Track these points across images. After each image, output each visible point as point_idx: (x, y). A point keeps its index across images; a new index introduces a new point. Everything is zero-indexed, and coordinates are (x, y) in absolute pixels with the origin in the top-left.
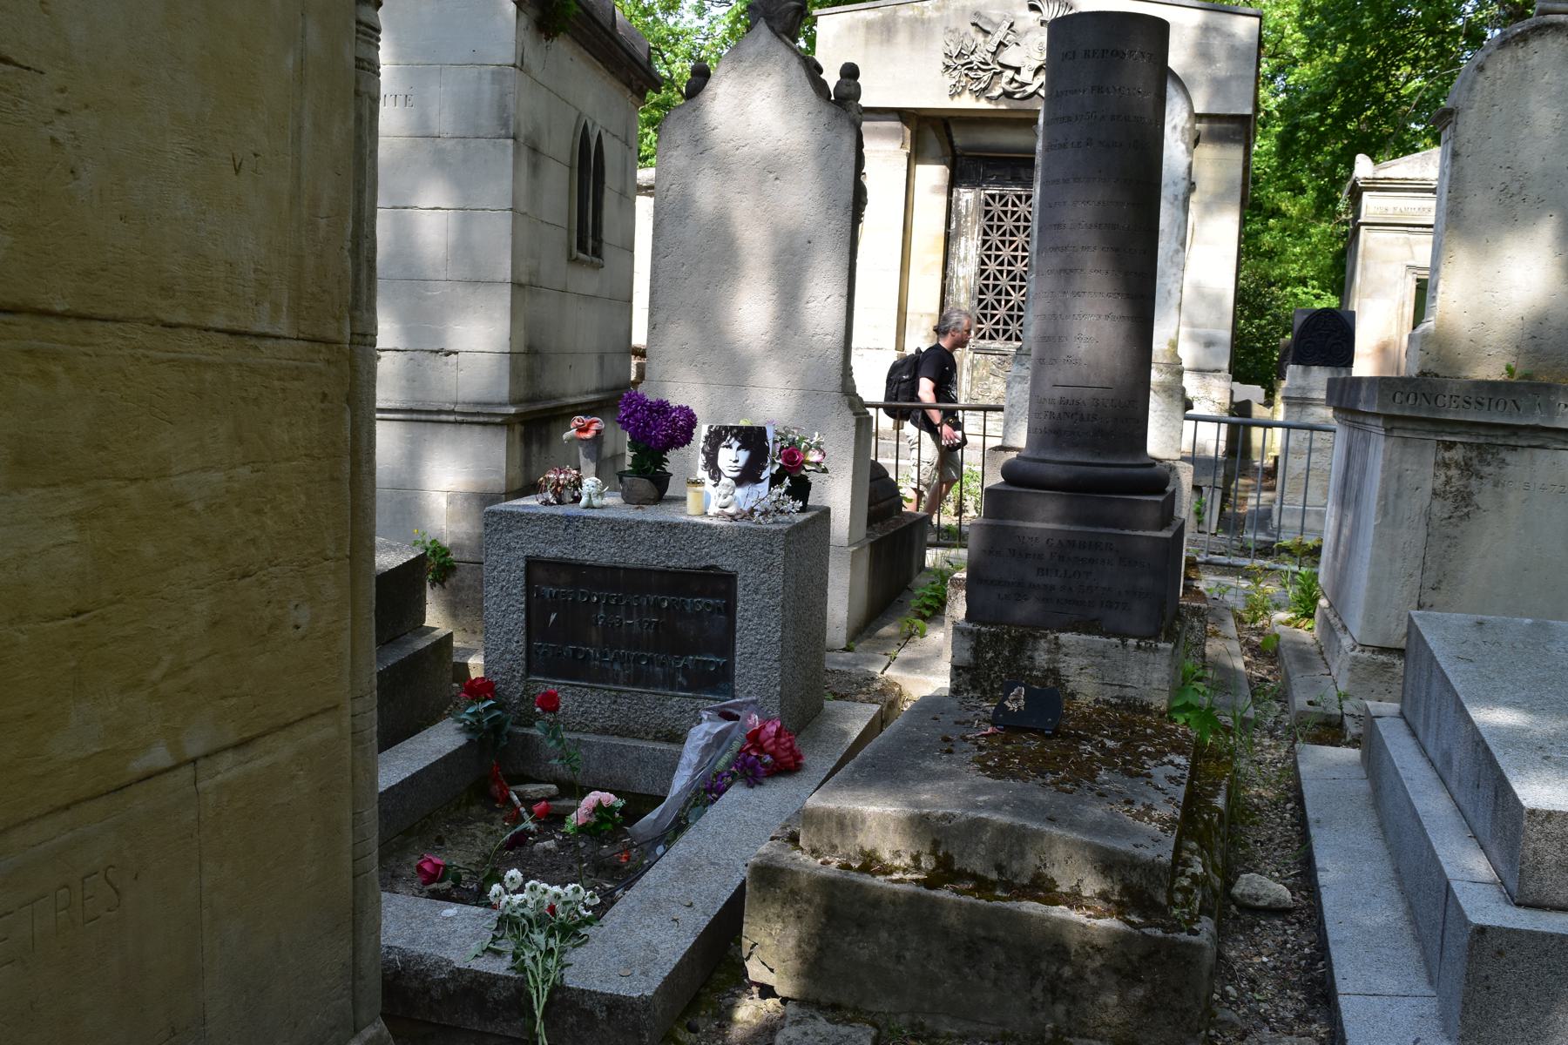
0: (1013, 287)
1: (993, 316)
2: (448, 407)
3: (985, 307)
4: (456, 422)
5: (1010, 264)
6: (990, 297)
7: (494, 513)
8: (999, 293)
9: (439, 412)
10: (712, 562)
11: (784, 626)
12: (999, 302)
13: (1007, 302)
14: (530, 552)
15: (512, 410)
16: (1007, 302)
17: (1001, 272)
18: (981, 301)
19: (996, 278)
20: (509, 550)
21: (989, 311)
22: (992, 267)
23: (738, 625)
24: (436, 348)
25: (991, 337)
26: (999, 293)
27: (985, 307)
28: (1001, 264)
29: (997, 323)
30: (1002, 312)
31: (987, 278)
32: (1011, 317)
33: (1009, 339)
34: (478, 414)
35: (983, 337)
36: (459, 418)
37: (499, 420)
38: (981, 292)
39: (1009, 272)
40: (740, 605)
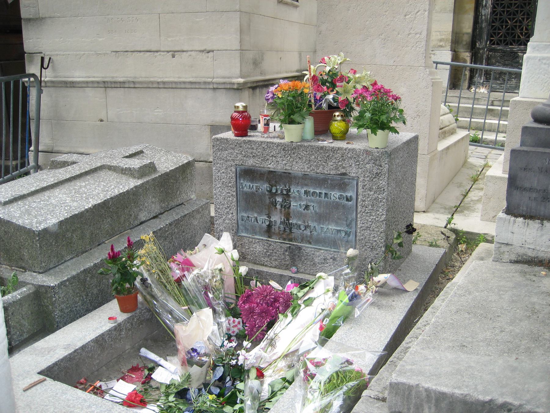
0: (510, 19)
1: (499, 33)
2: (210, 80)
3: (495, 29)
4: (214, 89)
5: (508, 7)
6: (497, 24)
7: (218, 139)
8: (502, 22)
9: (205, 83)
10: (343, 171)
11: (388, 211)
12: (502, 26)
13: (506, 26)
14: (237, 162)
15: (241, 80)
16: (506, 26)
17: (503, 12)
18: (493, 26)
19: (501, 15)
20: (226, 161)
21: (497, 31)
22: (499, 9)
23: (359, 209)
24: (202, 49)
25: (498, 44)
26: (502, 22)
27: (495, 29)
28: (504, 7)
29: (501, 37)
30: (503, 31)
31: (497, 15)
32: (508, 34)
33: (507, 44)
34: (224, 83)
35: (494, 44)
36: (215, 86)
37: (235, 87)
38: (493, 22)
39: (508, 11)
40: (360, 197)
